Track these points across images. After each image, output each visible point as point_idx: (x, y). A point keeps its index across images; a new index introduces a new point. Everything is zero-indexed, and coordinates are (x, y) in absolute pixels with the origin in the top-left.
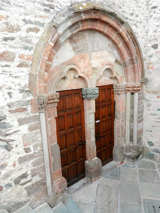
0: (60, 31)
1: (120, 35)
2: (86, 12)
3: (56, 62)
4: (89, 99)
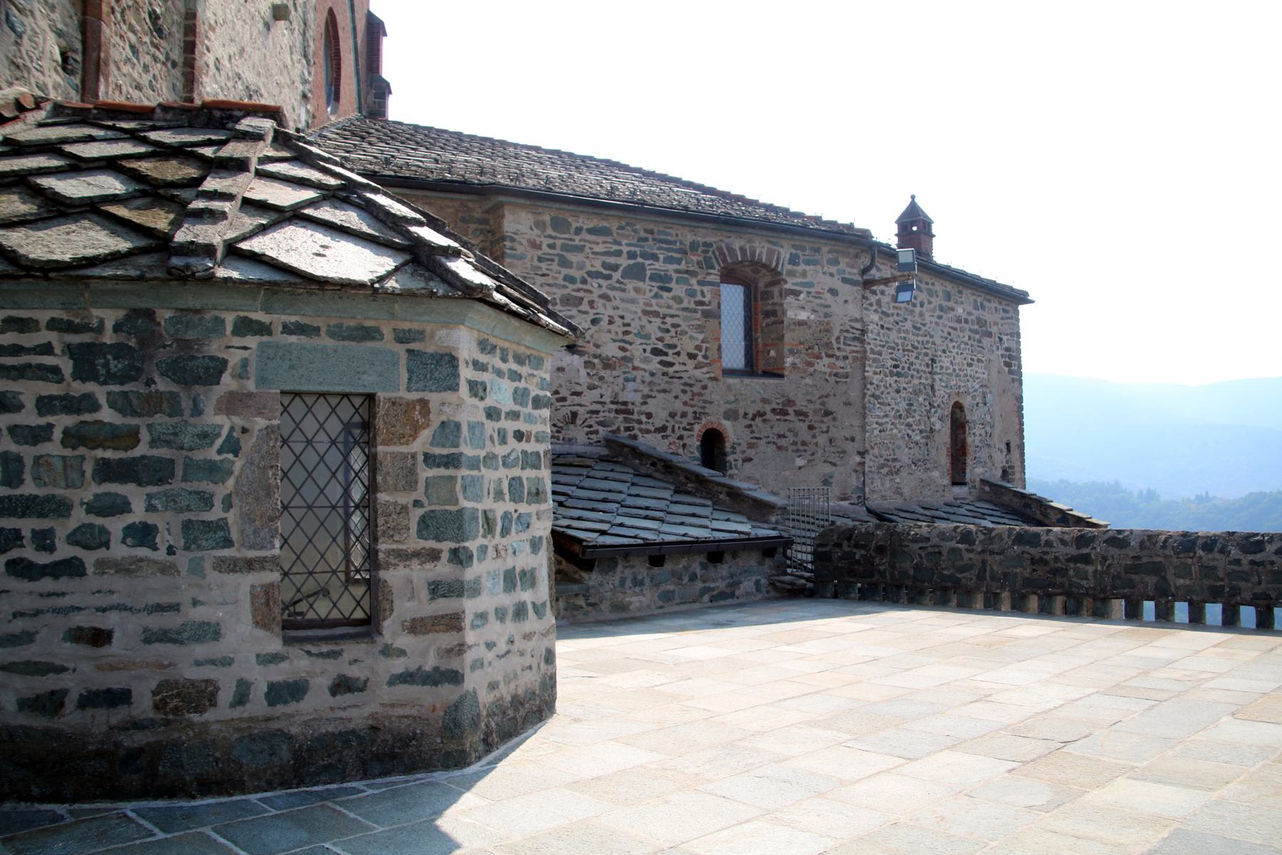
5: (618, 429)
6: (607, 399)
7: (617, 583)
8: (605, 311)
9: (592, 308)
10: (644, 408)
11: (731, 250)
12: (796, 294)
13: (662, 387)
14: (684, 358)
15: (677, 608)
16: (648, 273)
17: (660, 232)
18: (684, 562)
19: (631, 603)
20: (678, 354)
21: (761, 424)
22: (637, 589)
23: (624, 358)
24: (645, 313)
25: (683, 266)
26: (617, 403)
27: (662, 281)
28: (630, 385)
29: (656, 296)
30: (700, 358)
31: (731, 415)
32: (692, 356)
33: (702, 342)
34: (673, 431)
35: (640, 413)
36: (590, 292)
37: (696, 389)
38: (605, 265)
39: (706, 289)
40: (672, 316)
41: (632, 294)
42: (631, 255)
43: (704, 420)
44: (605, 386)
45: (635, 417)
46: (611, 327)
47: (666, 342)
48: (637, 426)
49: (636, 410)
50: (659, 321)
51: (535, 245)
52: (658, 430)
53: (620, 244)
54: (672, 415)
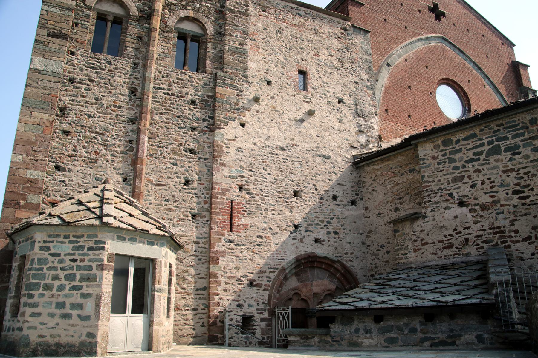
0: (287, 271)
1: (337, 269)
2: (304, 259)
3: (285, 289)
4: (311, 317)
5: (497, 243)
6: (486, 227)
7: (353, 330)
8: (478, 178)
9: (470, 179)
10: (513, 228)
13: (524, 212)
15: (399, 348)
16: (503, 149)
18: (405, 320)
19: (363, 343)
20: (532, 189)
22: (368, 335)
23: (494, 202)
24: (504, 172)
25: (527, 136)
26: (494, 228)
27: (514, 150)
28: (500, 216)
29: (510, 160)
35: (510, 231)
36: (468, 171)
38: (475, 154)
41: (495, 164)
42: (489, 143)
44: (484, 220)
45: (507, 234)
46: (483, 186)
47: (522, 184)
48: (509, 239)
49: (507, 230)
50: (515, 174)
51: (434, 158)
52: (525, 240)
53: (482, 139)
54: (534, 228)
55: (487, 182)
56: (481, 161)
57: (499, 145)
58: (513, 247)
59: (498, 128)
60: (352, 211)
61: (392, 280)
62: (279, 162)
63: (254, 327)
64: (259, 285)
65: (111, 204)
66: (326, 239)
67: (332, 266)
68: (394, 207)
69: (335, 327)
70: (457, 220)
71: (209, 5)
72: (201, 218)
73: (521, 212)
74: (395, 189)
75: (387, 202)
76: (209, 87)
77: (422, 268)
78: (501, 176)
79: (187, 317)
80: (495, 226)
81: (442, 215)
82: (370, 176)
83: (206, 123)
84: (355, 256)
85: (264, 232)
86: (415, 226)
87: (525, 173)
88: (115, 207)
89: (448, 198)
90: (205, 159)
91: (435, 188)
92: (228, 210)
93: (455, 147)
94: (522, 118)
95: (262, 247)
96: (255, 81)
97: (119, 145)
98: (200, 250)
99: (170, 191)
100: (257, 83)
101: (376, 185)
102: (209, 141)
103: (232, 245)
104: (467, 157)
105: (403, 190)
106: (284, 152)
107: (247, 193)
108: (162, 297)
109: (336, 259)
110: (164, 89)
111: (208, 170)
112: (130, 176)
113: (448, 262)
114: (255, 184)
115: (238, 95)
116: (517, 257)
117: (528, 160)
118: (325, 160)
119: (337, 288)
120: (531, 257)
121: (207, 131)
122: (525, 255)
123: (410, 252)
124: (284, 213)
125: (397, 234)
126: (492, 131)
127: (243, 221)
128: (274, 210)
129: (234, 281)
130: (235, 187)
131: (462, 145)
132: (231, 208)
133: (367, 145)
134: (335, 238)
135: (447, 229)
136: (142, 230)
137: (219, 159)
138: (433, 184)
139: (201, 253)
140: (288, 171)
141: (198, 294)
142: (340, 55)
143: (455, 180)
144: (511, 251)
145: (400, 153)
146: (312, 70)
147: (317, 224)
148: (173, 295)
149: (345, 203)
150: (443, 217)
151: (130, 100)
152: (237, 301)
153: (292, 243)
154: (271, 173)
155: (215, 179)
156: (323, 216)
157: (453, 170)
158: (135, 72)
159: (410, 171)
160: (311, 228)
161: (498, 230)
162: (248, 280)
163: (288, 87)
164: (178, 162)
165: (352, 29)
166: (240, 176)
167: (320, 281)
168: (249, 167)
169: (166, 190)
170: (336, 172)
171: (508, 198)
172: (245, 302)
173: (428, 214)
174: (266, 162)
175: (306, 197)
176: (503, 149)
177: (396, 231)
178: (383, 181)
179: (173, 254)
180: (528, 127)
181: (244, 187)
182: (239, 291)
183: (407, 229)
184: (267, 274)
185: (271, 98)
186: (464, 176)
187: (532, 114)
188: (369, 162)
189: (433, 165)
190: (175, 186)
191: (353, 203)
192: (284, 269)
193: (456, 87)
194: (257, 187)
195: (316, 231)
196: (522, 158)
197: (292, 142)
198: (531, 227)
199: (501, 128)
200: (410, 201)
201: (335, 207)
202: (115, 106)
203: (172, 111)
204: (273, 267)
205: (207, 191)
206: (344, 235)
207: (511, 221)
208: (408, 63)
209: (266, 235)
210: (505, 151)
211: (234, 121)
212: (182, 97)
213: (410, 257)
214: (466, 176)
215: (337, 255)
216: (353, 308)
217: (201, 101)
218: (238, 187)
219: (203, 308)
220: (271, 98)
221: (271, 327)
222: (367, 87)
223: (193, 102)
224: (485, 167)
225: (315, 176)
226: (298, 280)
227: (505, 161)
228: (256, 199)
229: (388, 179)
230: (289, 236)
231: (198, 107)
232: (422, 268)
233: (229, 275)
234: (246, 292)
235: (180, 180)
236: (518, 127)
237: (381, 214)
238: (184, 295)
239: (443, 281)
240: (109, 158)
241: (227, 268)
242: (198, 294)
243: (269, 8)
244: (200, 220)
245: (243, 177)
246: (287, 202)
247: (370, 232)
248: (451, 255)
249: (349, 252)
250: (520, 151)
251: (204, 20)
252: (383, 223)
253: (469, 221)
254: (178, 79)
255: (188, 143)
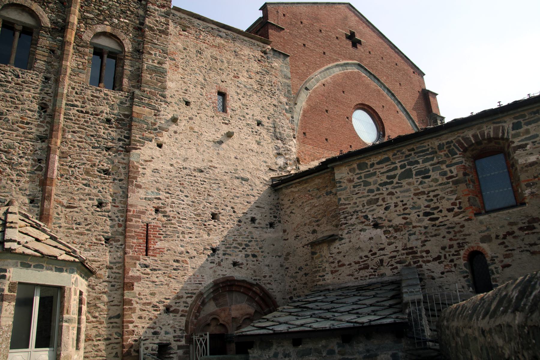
0: (205, 296)
2: (222, 283)
3: (203, 314)
5: (410, 263)
6: (400, 248)
7: (271, 355)
9: (384, 201)
10: (424, 248)
11: (466, 139)
12: (523, 147)
14: (445, 212)
16: (414, 172)
17: (417, 148)
18: (324, 342)
20: (441, 211)
21: (512, 240)
23: (406, 223)
24: (415, 194)
25: (435, 160)
26: (407, 249)
27: (424, 174)
28: (412, 237)
29: (421, 183)
30: (456, 210)
31: (486, 239)
32: (449, 210)
33: (456, 200)
34: (445, 258)
35: (422, 252)
36: (382, 194)
37: (457, 229)
38: (388, 177)
39: (452, 168)
40: (433, 191)
41: (407, 187)
42: (402, 167)
43: (466, 247)
44: (397, 241)
45: (419, 254)
47: (432, 206)
48: (420, 260)
49: (419, 250)
50: (425, 197)
51: (350, 181)
52: (435, 259)
53: (395, 163)
54: (443, 248)
55: (400, 204)
56: (394, 185)
57: (410, 169)
58: (425, 267)
59: (410, 153)
60: (270, 234)
61: (310, 302)
62: (197, 185)
63: (171, 355)
64: (176, 311)
65: (15, 228)
66: (245, 262)
67: (251, 290)
68: (312, 229)
69: (253, 352)
70: (372, 241)
71: (127, 21)
72: (115, 242)
73: (431, 233)
74: (313, 211)
75: (305, 225)
76: (126, 105)
77: (339, 289)
78: (412, 199)
79: (99, 347)
80: (408, 247)
81: (358, 237)
82: (288, 198)
83: (121, 143)
84: (273, 279)
85: (181, 255)
86: (332, 247)
87: (435, 196)
88: (19, 232)
89: (364, 220)
90: (120, 180)
91: (351, 211)
92: (143, 233)
93: (370, 171)
94: (431, 143)
95: (179, 271)
96: (173, 101)
97: (26, 165)
98: (114, 275)
99: (81, 213)
100: (176, 103)
101: (294, 207)
102: (125, 161)
103: (148, 270)
104: (381, 180)
105: (320, 212)
106: (202, 174)
107: (164, 216)
108: (70, 328)
109: (254, 282)
110: (77, 106)
111: (123, 191)
112: (38, 197)
113: (364, 283)
114: (172, 207)
115: (155, 115)
116: (428, 276)
117: (436, 184)
118: (244, 182)
119: (256, 311)
120: (441, 275)
121: (122, 151)
122: (436, 274)
123: (327, 274)
124: (202, 236)
125: (315, 256)
126: (404, 155)
127: (159, 245)
128: (191, 233)
129: (149, 307)
130: (151, 210)
131: (376, 169)
132: (147, 231)
133: (285, 167)
134: (253, 261)
135: (362, 251)
136: (50, 256)
137: (134, 181)
138: (349, 206)
139: (115, 278)
140: (206, 193)
141: (111, 323)
142: (259, 77)
143: (370, 202)
144: (422, 271)
145: (317, 176)
146: (231, 92)
147: (235, 247)
148: (83, 325)
149: (263, 225)
150: (359, 239)
151: (40, 116)
152: (153, 328)
153: (210, 267)
154: (189, 195)
155: (130, 201)
156: (241, 239)
157: (368, 192)
158: (46, 87)
159: (327, 194)
160: (229, 251)
161: (410, 251)
162: (164, 306)
163: (207, 108)
164: (91, 183)
165: (272, 53)
166: (156, 198)
167: (238, 306)
168: (165, 189)
169: (77, 212)
170: (254, 194)
171: (419, 219)
172: (161, 329)
173: (345, 236)
174: (183, 184)
175: (224, 220)
176: (414, 172)
177: (313, 253)
178: (301, 204)
179: (84, 280)
180: (436, 153)
181: (160, 210)
182: (155, 318)
183: (325, 250)
184: (184, 300)
185: (190, 118)
186: (378, 199)
187: (440, 140)
188: (287, 184)
189: (349, 187)
190: (87, 208)
191: (271, 225)
192: (201, 294)
193: (372, 112)
194: (174, 209)
195: (234, 254)
196: (432, 181)
197: (210, 164)
198: (440, 247)
199: (412, 153)
200: (327, 224)
201: (253, 230)
202: (23, 123)
203: (85, 129)
204: (191, 292)
205: (122, 214)
206: (263, 258)
207: (422, 242)
208: (326, 88)
209: (183, 259)
210: (416, 175)
211: (151, 141)
212: (97, 115)
213: (328, 279)
214: (380, 199)
215: (255, 278)
216: (271, 332)
217: (117, 120)
218: (154, 209)
219: (116, 337)
220: (190, 118)
221: (189, 354)
222: (286, 110)
223: (108, 121)
224: (397, 190)
225: (233, 199)
226: (217, 305)
227: (416, 184)
228: (173, 222)
229: (306, 202)
230: (207, 260)
231: (114, 125)
232: (339, 289)
233: (145, 301)
234: (162, 318)
235: (93, 202)
236: (428, 152)
237: (299, 236)
238: (95, 324)
239: (360, 302)
240: (15, 177)
241: (142, 294)
242: (111, 323)
243: (189, 27)
244: (114, 244)
245: (159, 199)
246: (205, 225)
247: (288, 254)
248: (366, 276)
249: (268, 275)
250: (429, 174)
251: (122, 36)
252: (301, 245)
253: (383, 242)
254: (92, 96)
255: (102, 163)
